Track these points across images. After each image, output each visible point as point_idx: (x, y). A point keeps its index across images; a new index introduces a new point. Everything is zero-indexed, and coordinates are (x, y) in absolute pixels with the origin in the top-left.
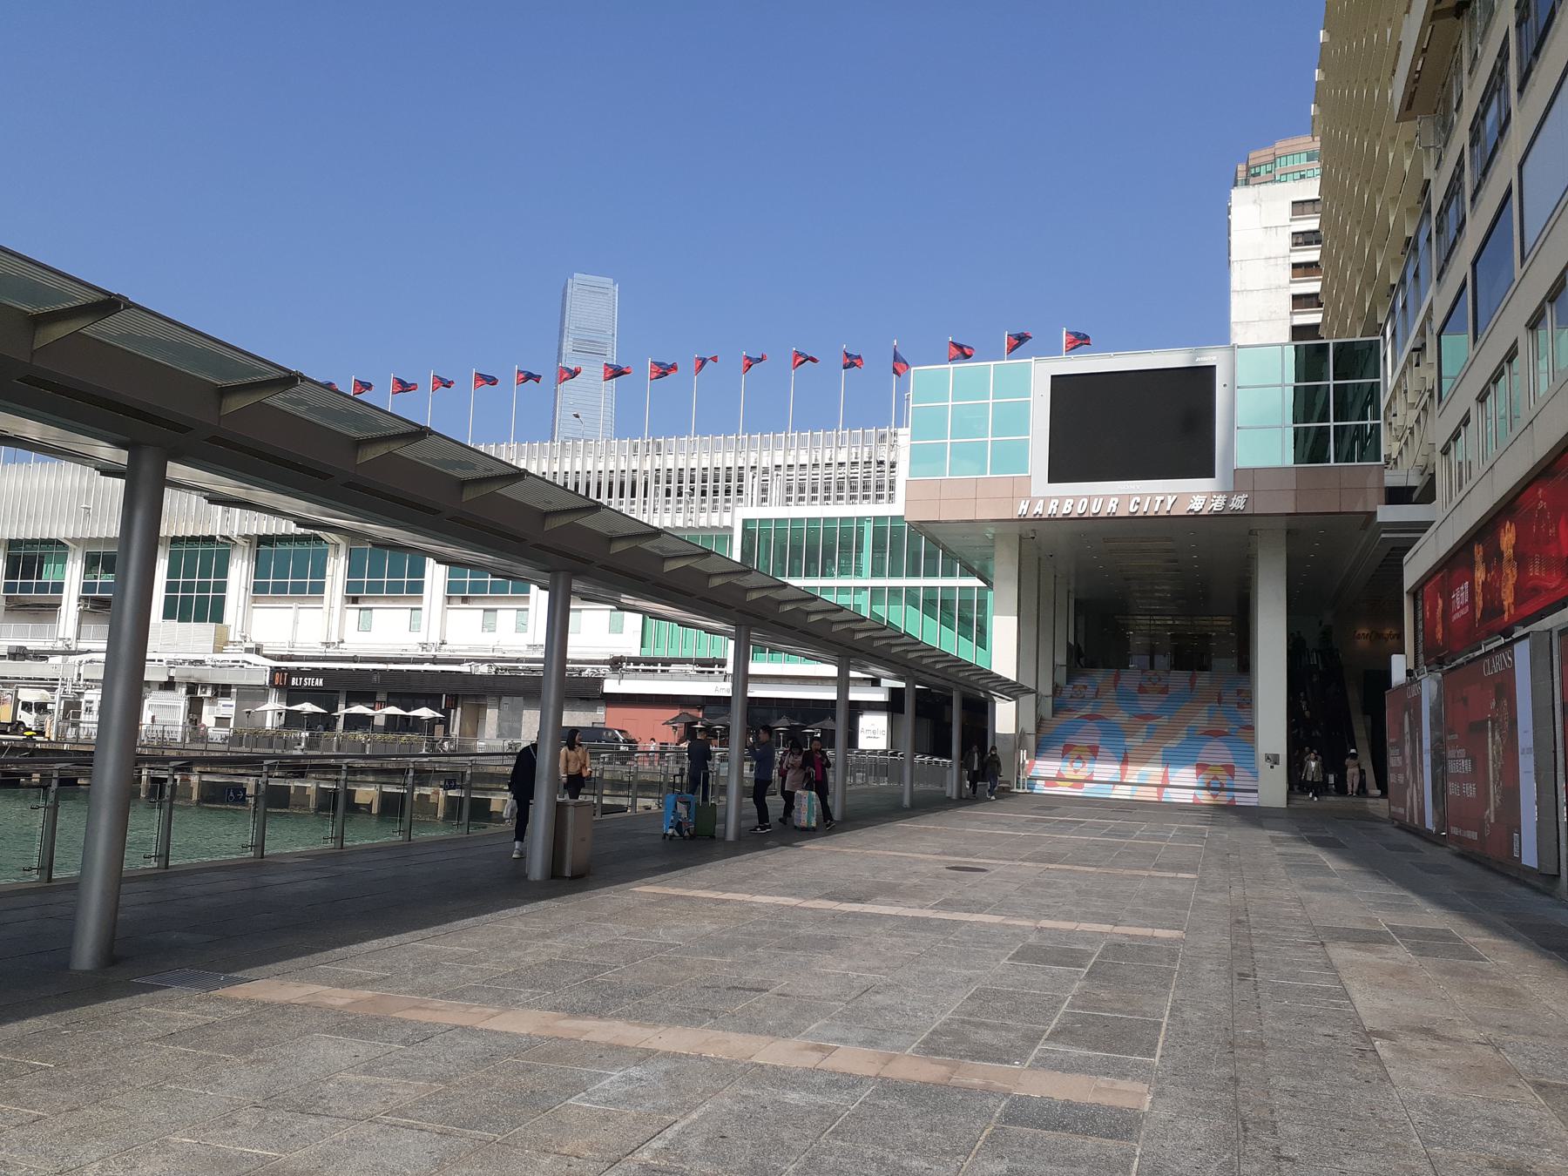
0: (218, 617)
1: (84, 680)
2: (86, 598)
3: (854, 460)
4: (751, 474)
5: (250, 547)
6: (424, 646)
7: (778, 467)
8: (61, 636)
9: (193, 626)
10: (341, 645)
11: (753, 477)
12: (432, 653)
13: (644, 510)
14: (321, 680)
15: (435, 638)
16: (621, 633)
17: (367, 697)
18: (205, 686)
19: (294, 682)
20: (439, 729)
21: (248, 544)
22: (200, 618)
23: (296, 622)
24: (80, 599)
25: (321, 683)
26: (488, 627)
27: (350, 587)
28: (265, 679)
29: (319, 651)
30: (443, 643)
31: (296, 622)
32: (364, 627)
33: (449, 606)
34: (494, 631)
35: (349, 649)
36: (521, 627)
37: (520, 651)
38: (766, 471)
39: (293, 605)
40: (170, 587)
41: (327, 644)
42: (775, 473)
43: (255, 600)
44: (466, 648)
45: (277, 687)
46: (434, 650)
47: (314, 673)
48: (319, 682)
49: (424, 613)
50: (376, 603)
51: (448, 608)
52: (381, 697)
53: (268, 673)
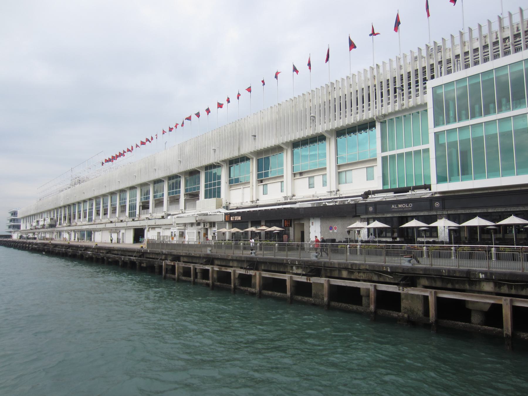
0: (219, 196)
1: (177, 224)
2: (187, 194)
3: (516, 33)
4: (439, 66)
5: (226, 166)
6: (285, 198)
7: (458, 56)
8: (181, 209)
9: (212, 199)
10: (257, 202)
11: (441, 68)
12: (289, 201)
13: (376, 107)
14: (240, 217)
15: (290, 194)
16: (374, 179)
17: (256, 223)
18: (207, 223)
19: (232, 219)
20: (285, 237)
21: (225, 165)
22: (214, 197)
23: (243, 194)
24: (185, 195)
25: (240, 219)
26: (311, 186)
27: (259, 176)
28: (222, 218)
29: (249, 204)
30: (294, 196)
31: (243, 194)
32: (265, 193)
33: (295, 178)
34: (314, 187)
35: (260, 203)
36: (324, 184)
37: (325, 196)
38: (449, 61)
39: (242, 187)
40: (206, 186)
41: (252, 202)
42: (456, 60)
43: (231, 187)
44: (302, 197)
45: (229, 221)
46: (289, 199)
47: (238, 214)
48: (239, 218)
49: (285, 183)
50: (269, 181)
51: (294, 179)
52: (263, 223)
53: (224, 215)
